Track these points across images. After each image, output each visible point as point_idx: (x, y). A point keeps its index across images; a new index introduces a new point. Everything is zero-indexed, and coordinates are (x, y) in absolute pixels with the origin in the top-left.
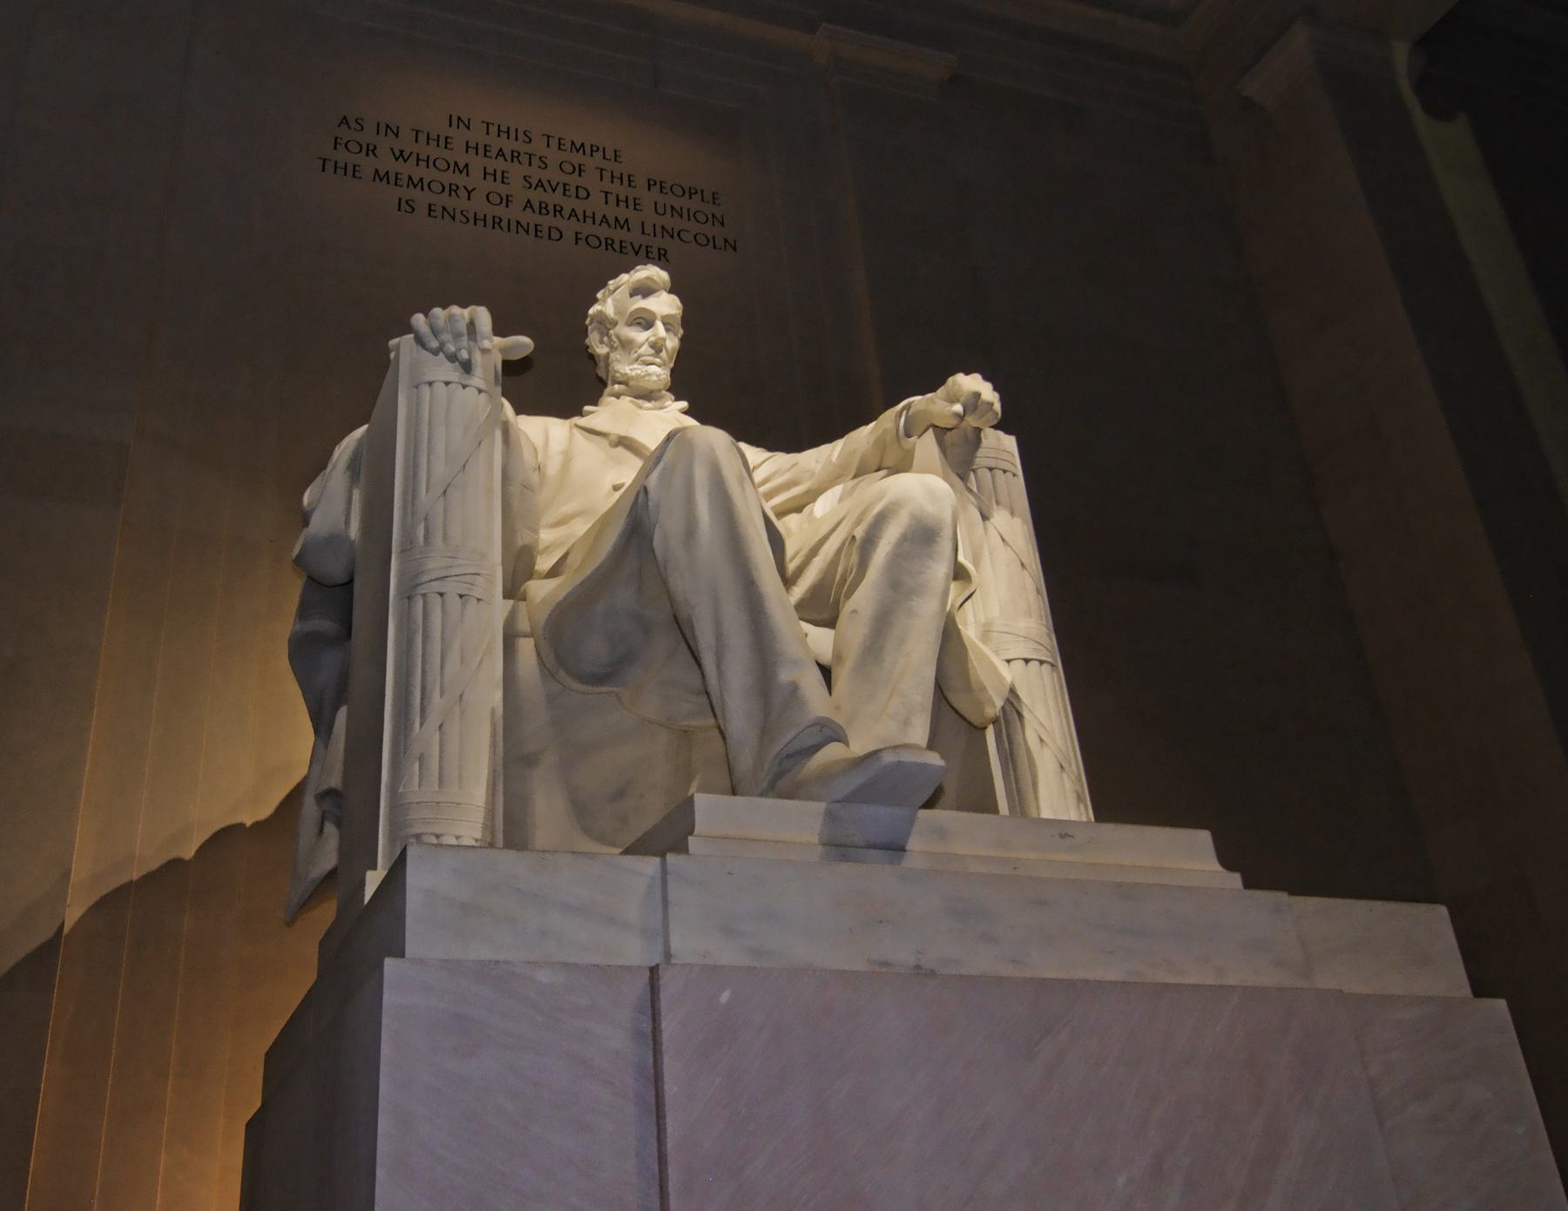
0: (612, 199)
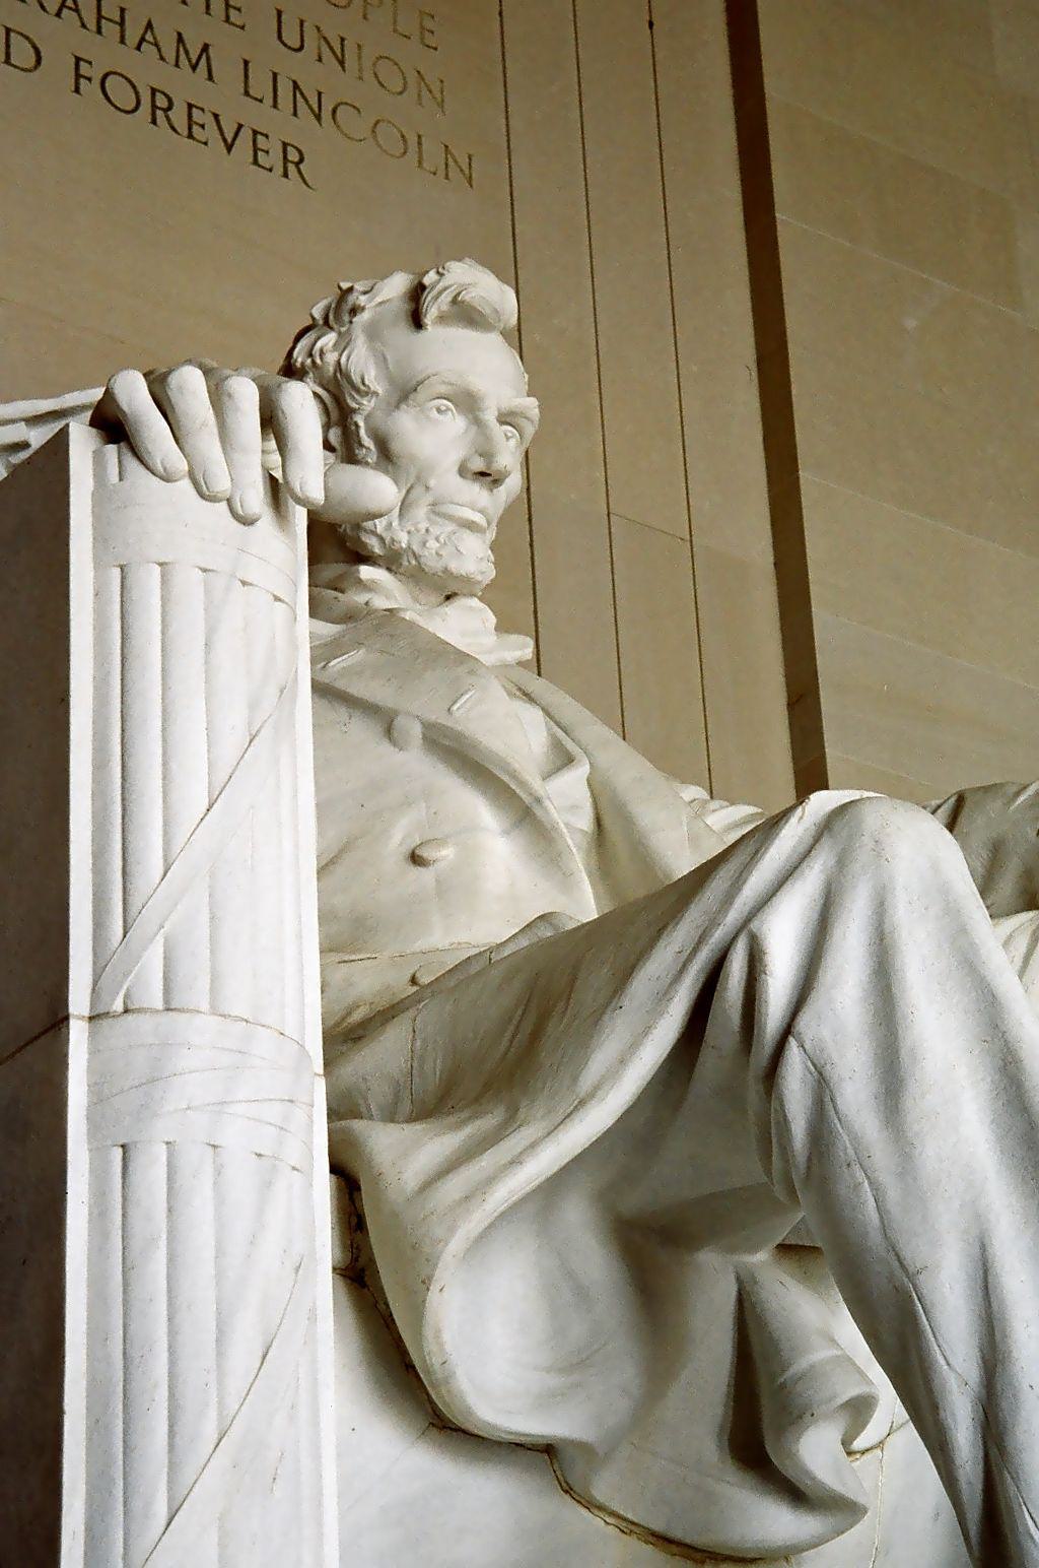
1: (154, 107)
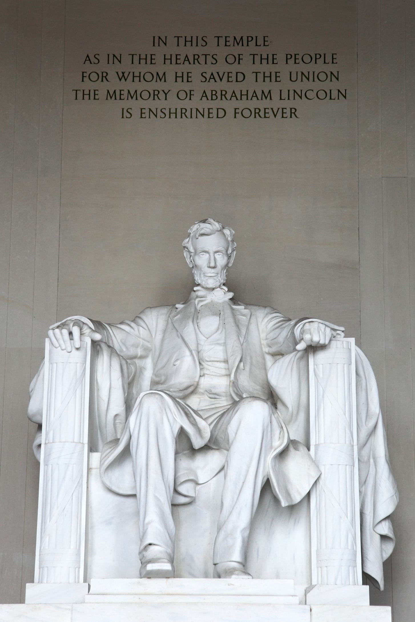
0: (260, 77)
1: (255, 113)
